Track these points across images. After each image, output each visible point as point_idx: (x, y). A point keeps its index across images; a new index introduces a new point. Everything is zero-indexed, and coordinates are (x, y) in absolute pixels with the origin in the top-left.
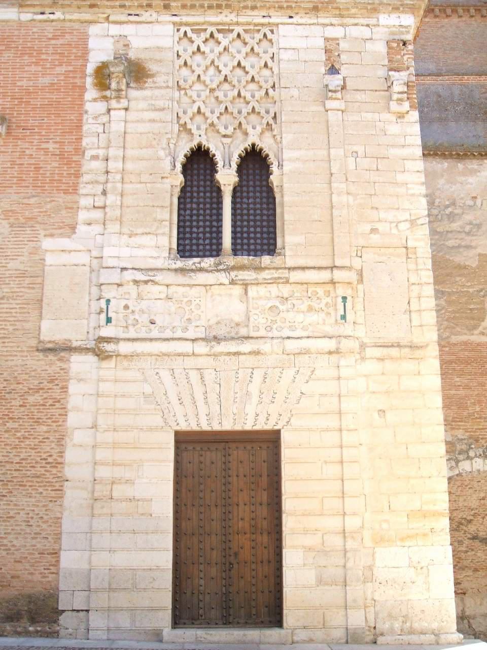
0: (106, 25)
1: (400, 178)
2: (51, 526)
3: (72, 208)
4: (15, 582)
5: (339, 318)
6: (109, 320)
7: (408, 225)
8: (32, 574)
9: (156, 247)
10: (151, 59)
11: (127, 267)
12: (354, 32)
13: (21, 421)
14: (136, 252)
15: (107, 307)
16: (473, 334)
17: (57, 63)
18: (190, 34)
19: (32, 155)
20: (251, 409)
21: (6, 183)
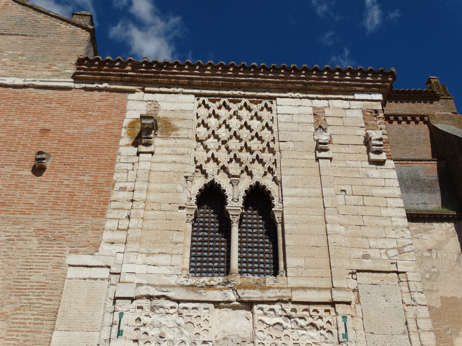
1: (384, 212)
5: (341, 337)
7: (396, 252)
9: (170, 266)
10: (175, 118)
11: (142, 282)
15: (120, 320)
17: (100, 118)
19: (69, 185)
21: (41, 206)
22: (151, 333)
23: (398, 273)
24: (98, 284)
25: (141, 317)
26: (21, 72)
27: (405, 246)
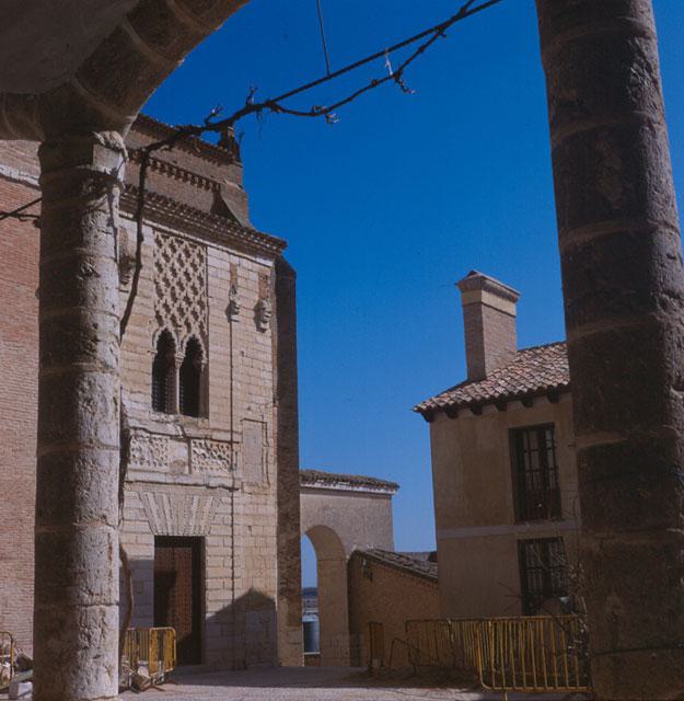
18: (160, 238)
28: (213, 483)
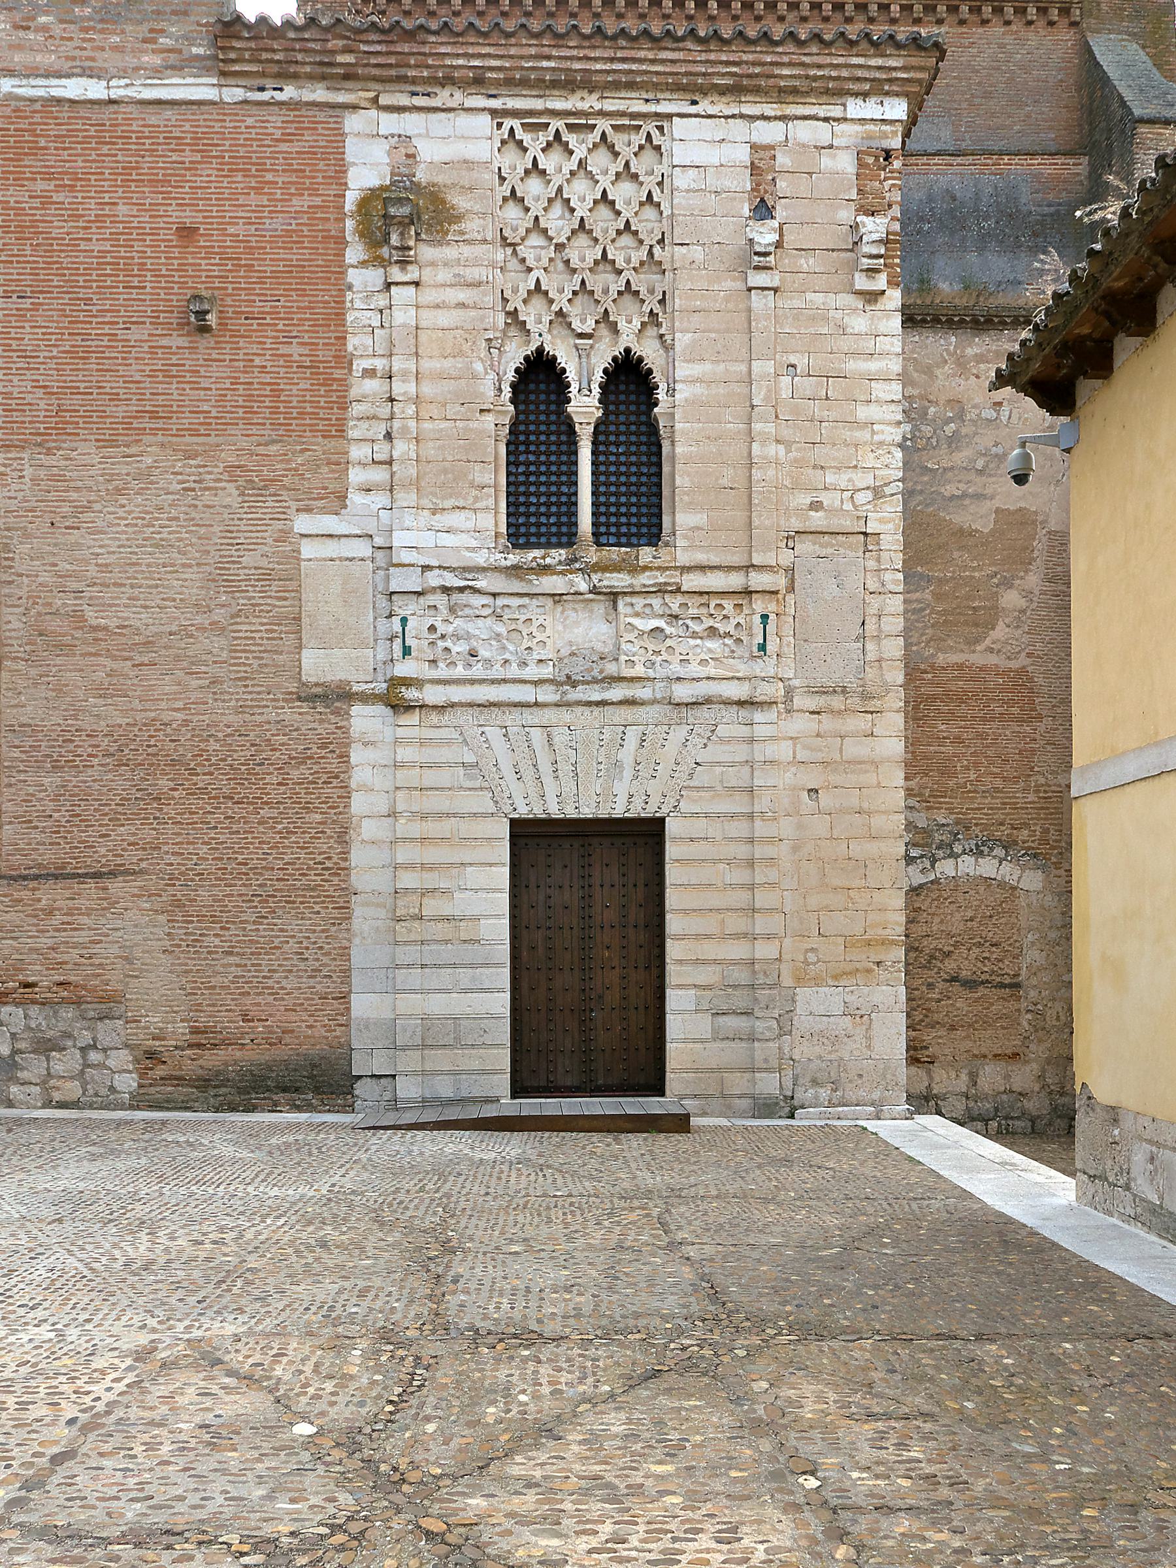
0: (373, 113)
1: (863, 412)
2: (335, 959)
3: (338, 464)
4: (287, 1039)
5: (755, 649)
6: (407, 651)
7: (869, 495)
8: (310, 1027)
12: (804, 132)
13: (281, 807)
14: (447, 540)
15: (404, 630)
16: (974, 652)
18: (519, 134)
19: (265, 367)
20: (622, 788)
21: (225, 418)
22: (456, 649)
23: (865, 534)
24: (355, 567)
25: (436, 624)
26: (93, 59)
27: (886, 485)
28: (682, 692)
